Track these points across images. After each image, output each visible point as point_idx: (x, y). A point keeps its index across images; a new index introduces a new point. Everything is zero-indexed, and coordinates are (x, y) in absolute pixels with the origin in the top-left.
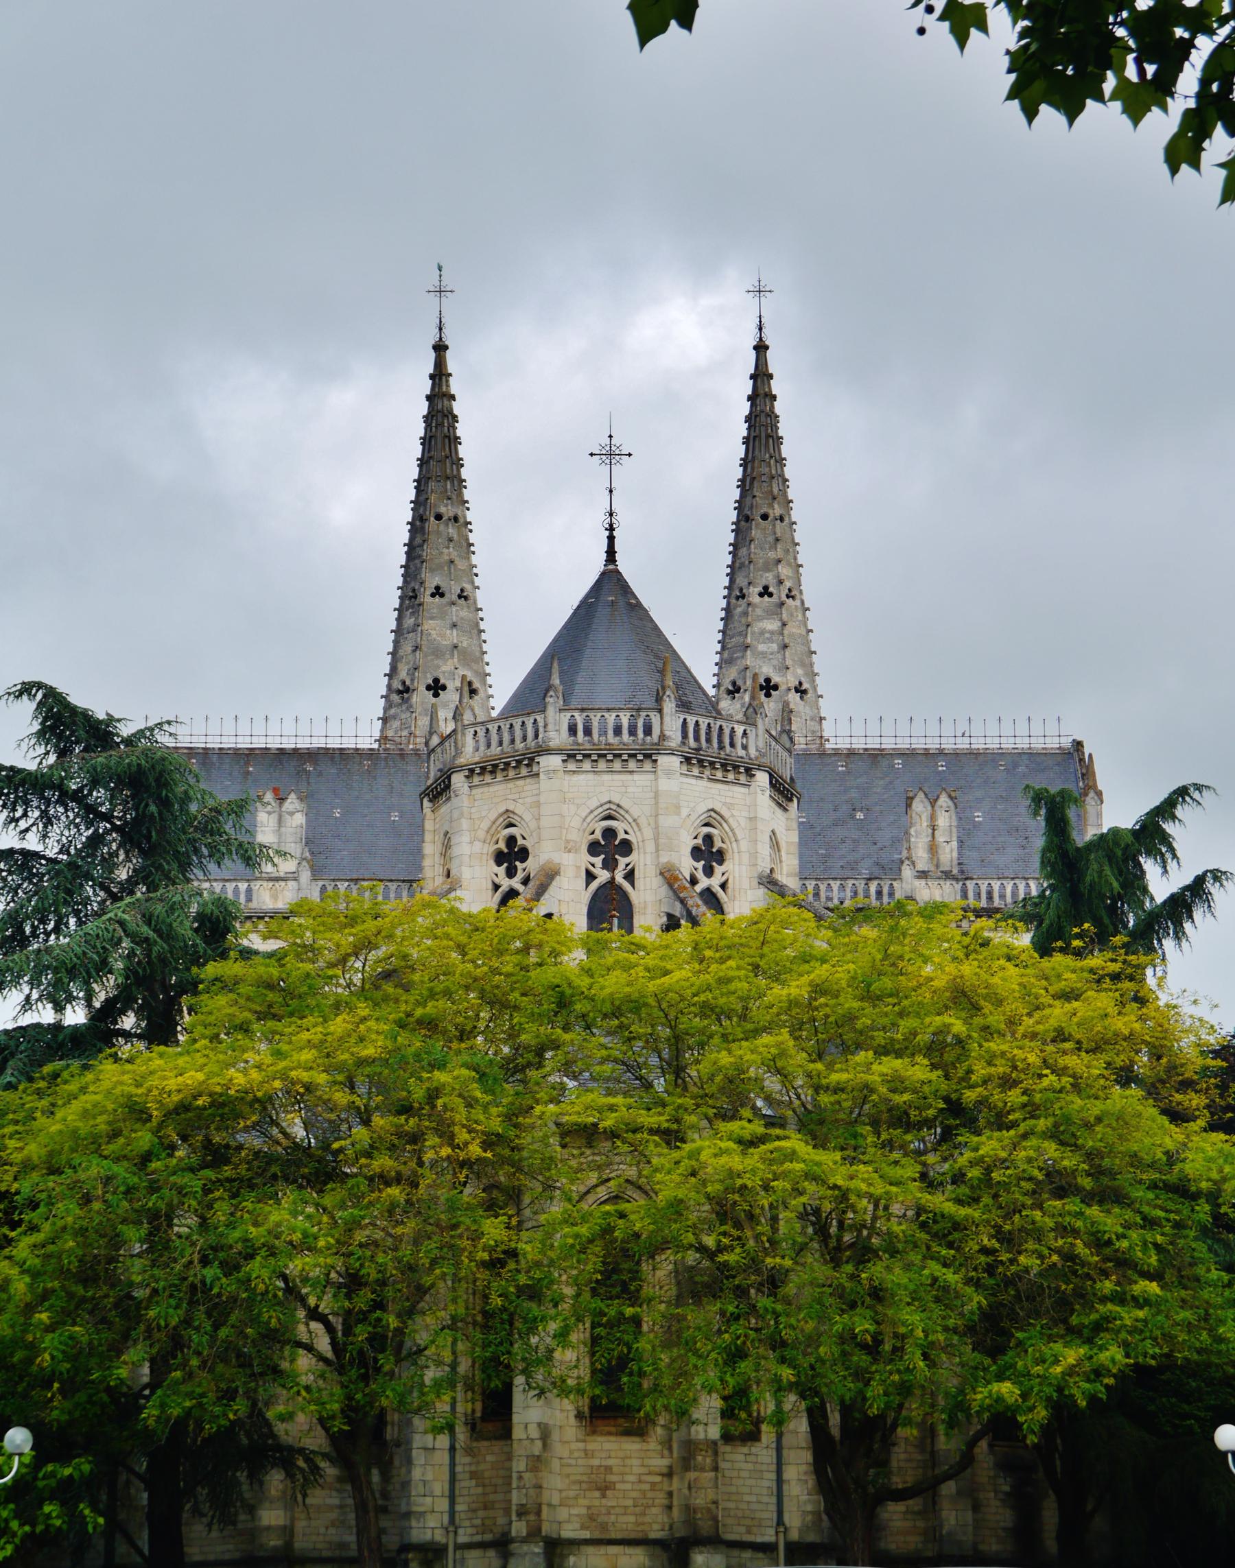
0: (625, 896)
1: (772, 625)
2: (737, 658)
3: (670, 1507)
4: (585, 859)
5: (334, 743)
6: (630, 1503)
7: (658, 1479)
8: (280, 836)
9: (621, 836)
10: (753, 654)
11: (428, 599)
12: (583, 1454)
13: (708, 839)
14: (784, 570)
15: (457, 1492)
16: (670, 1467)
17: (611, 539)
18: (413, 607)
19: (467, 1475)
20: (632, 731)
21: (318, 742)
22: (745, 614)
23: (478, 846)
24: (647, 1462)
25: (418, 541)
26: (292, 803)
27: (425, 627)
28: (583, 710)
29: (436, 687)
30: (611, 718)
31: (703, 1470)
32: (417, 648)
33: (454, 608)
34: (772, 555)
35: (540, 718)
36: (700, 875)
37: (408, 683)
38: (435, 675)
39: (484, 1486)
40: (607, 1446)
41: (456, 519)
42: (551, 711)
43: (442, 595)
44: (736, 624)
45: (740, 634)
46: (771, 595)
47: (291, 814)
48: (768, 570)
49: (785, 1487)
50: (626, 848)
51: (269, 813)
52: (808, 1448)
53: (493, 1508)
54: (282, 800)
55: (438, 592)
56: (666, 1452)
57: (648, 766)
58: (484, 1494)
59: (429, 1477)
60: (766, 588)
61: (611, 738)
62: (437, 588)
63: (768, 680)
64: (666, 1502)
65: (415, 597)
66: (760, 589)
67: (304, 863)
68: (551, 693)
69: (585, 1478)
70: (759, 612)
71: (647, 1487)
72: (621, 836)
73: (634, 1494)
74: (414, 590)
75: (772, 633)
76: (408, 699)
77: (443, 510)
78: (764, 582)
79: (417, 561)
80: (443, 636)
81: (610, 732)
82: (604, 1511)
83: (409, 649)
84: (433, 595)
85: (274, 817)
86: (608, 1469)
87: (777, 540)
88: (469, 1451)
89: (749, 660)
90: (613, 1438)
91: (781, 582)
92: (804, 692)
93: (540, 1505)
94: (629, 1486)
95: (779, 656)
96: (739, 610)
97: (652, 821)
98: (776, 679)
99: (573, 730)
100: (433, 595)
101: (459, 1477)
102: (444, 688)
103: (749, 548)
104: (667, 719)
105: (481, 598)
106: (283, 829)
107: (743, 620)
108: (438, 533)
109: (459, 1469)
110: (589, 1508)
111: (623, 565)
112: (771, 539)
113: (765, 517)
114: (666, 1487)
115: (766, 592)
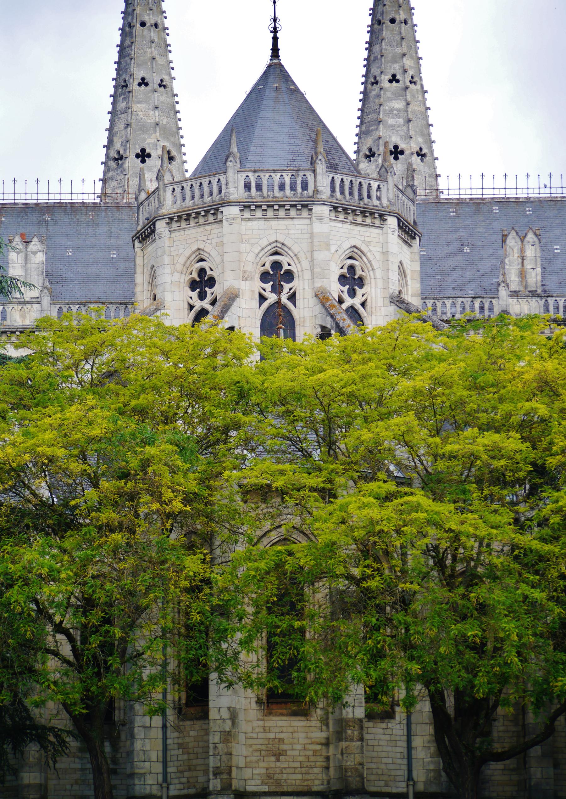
0: (289, 312)
1: (399, 104)
2: (372, 131)
3: (327, 768)
4: (258, 285)
5: (66, 199)
6: (298, 765)
7: (319, 747)
8: (26, 270)
9: (285, 267)
10: (384, 127)
11: (136, 87)
12: (262, 730)
13: (352, 268)
14: (408, 62)
15: (168, 759)
16: (328, 739)
17: (275, 39)
18: (124, 94)
19: (176, 746)
20: (293, 187)
21: (54, 198)
22: (378, 96)
23: (176, 276)
24: (310, 735)
25: (128, 42)
26: (35, 245)
27: (134, 109)
28: (255, 171)
29: (143, 156)
30: (276, 177)
31: (352, 740)
32: (128, 125)
33: (156, 95)
34: (398, 50)
35: (222, 178)
36: (345, 296)
37: (122, 152)
38: (143, 145)
39: (188, 754)
40: (280, 724)
41: (156, 25)
42: (230, 172)
43: (147, 84)
44: (372, 104)
45: (374, 111)
46: (398, 81)
47: (35, 253)
48: (396, 62)
49: (413, 752)
50: (289, 276)
51: (18, 253)
52: (431, 724)
53: (195, 770)
54: (27, 242)
55: (143, 82)
56: (324, 728)
57: (305, 213)
58: (189, 760)
59: (148, 747)
60: (394, 76)
61: (277, 193)
62: (143, 79)
63: (396, 147)
64: (324, 764)
65: (126, 86)
66: (390, 77)
67: (45, 291)
68: (231, 159)
69: (264, 747)
70: (389, 94)
71: (311, 753)
72: (285, 267)
73: (301, 759)
74: (125, 81)
75: (399, 110)
76: (122, 164)
77: (146, 18)
78: (392, 72)
79: (127, 59)
80: (148, 116)
81: (276, 188)
82: (278, 771)
83: (122, 126)
84: (140, 85)
85: (22, 255)
86: (281, 740)
87: (403, 39)
88: (177, 728)
89: (382, 131)
90: (285, 718)
91: (405, 71)
92: (423, 156)
93: (231, 767)
94: (296, 753)
95: (405, 128)
96: (374, 93)
97: (308, 255)
98: (402, 146)
99: (247, 187)
100: (140, 85)
101: (169, 747)
102: (149, 156)
103: (381, 46)
104: (319, 178)
105: (177, 86)
106: (29, 265)
107: (377, 101)
108: (143, 36)
109: (169, 741)
110: (267, 769)
111: (285, 58)
112: (398, 38)
113: (393, 21)
114: (325, 754)
115: (394, 79)
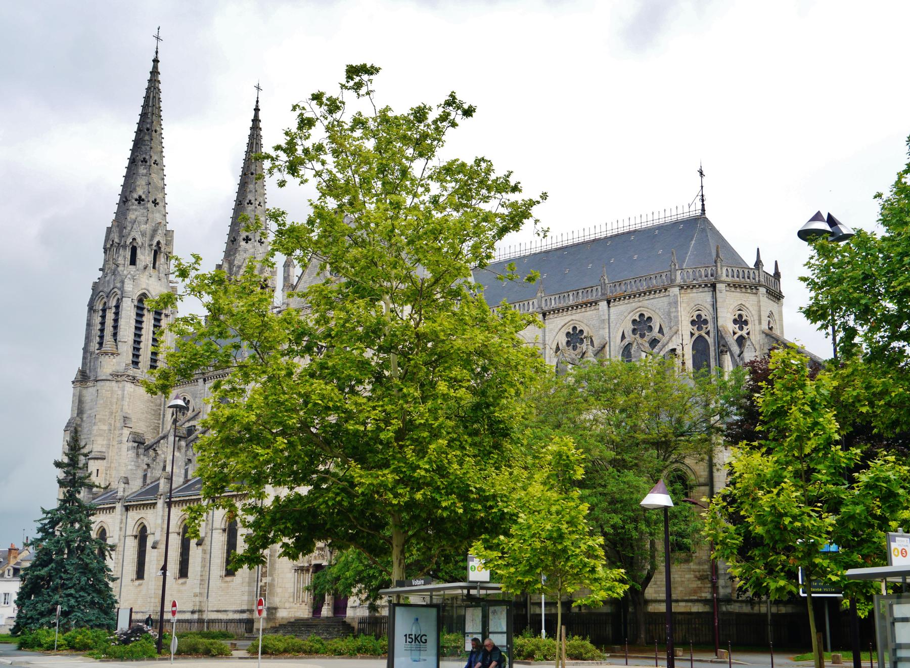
27: (152, 176)
37: (143, 197)
74: (144, 159)
76: (144, 204)
79: (148, 148)
83: (144, 183)
84: (154, 163)
100: (154, 163)
